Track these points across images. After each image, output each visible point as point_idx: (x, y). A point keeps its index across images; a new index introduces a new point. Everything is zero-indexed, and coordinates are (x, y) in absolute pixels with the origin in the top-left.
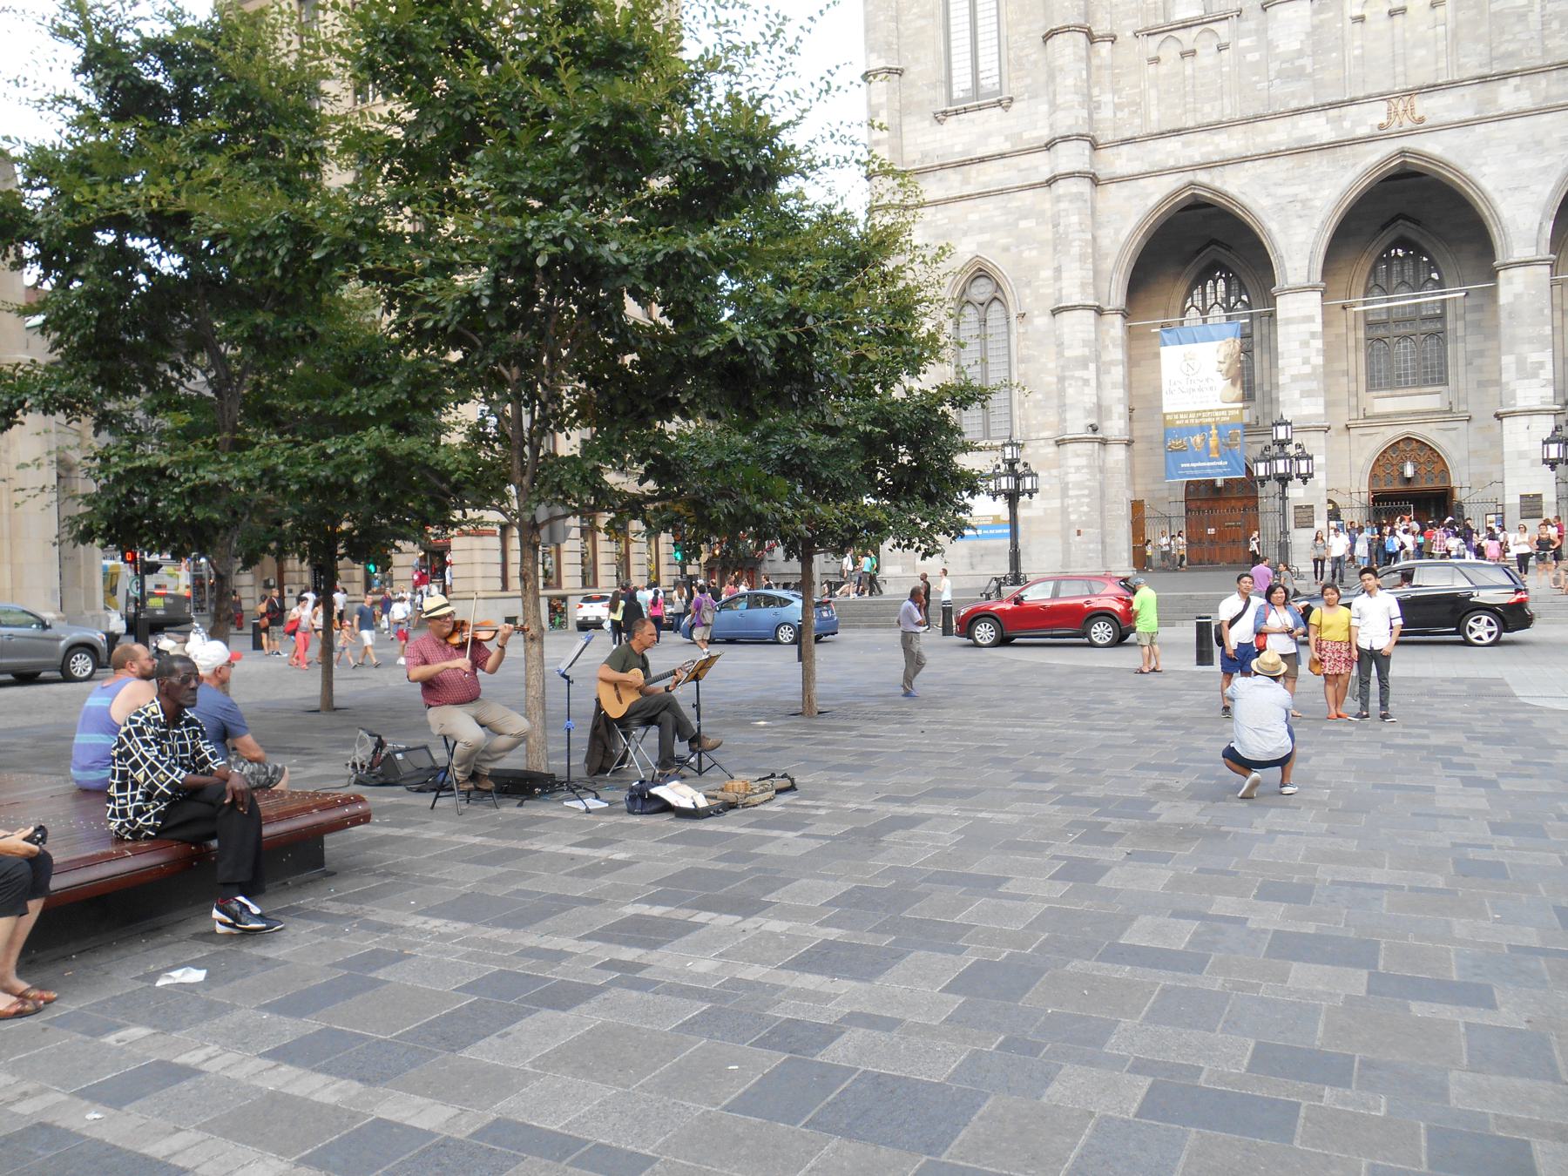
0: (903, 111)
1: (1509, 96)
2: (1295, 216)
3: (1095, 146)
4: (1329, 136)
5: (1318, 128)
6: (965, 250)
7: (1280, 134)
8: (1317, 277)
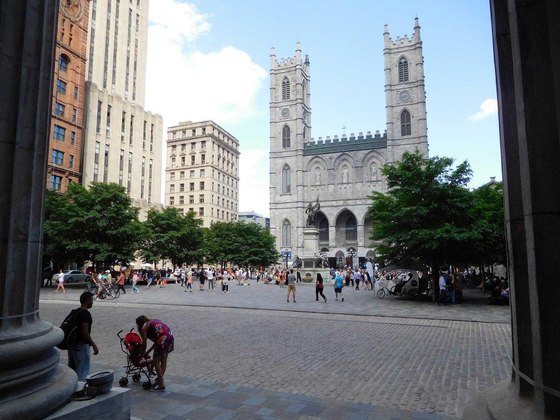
0: (276, 194)
1: (359, 202)
2: (332, 215)
3: (304, 202)
4: (336, 205)
5: (334, 203)
6: (285, 216)
7: (329, 203)
8: (335, 225)
